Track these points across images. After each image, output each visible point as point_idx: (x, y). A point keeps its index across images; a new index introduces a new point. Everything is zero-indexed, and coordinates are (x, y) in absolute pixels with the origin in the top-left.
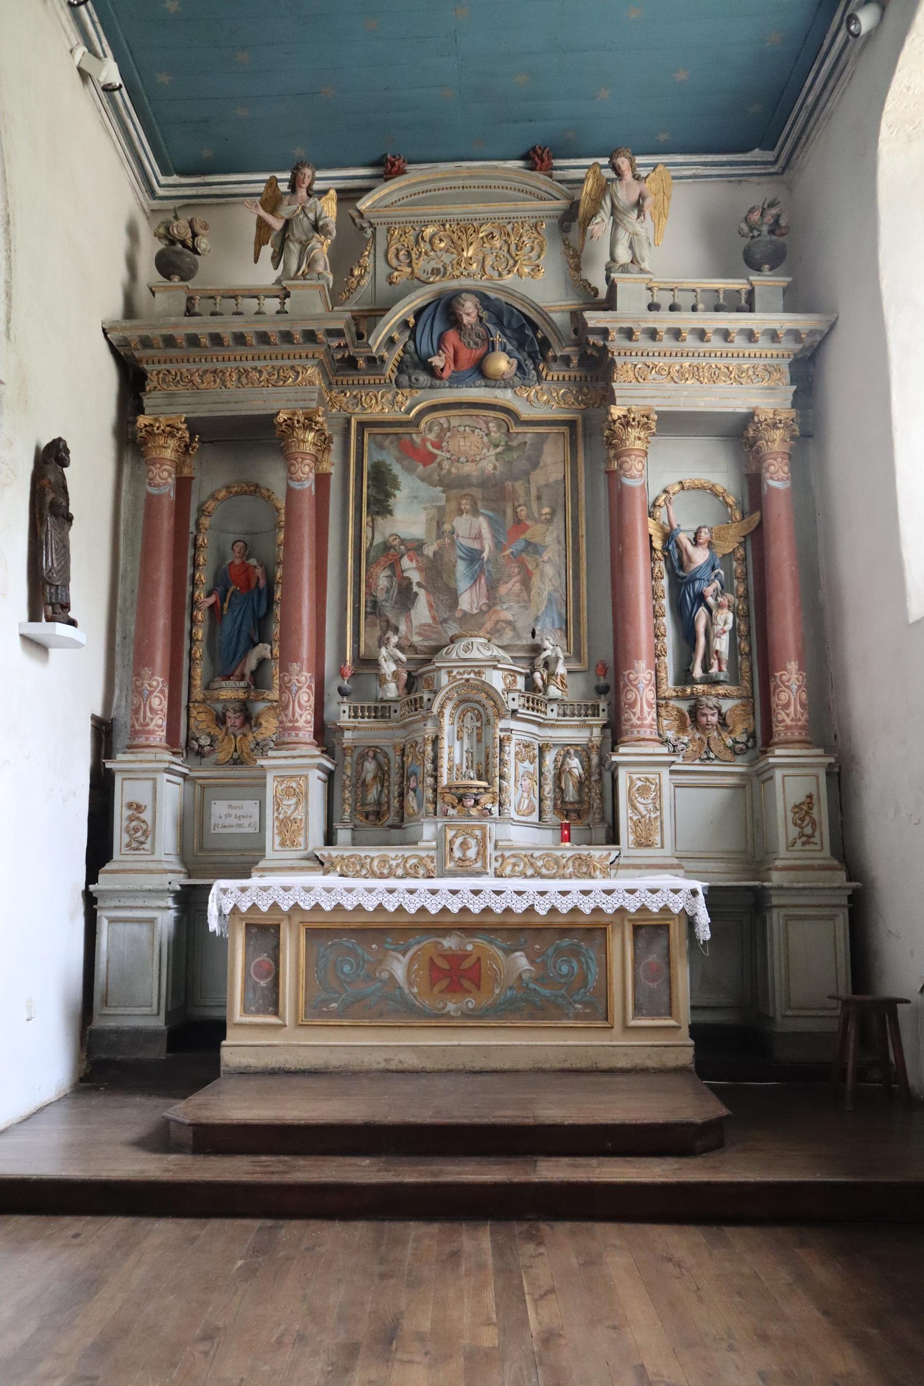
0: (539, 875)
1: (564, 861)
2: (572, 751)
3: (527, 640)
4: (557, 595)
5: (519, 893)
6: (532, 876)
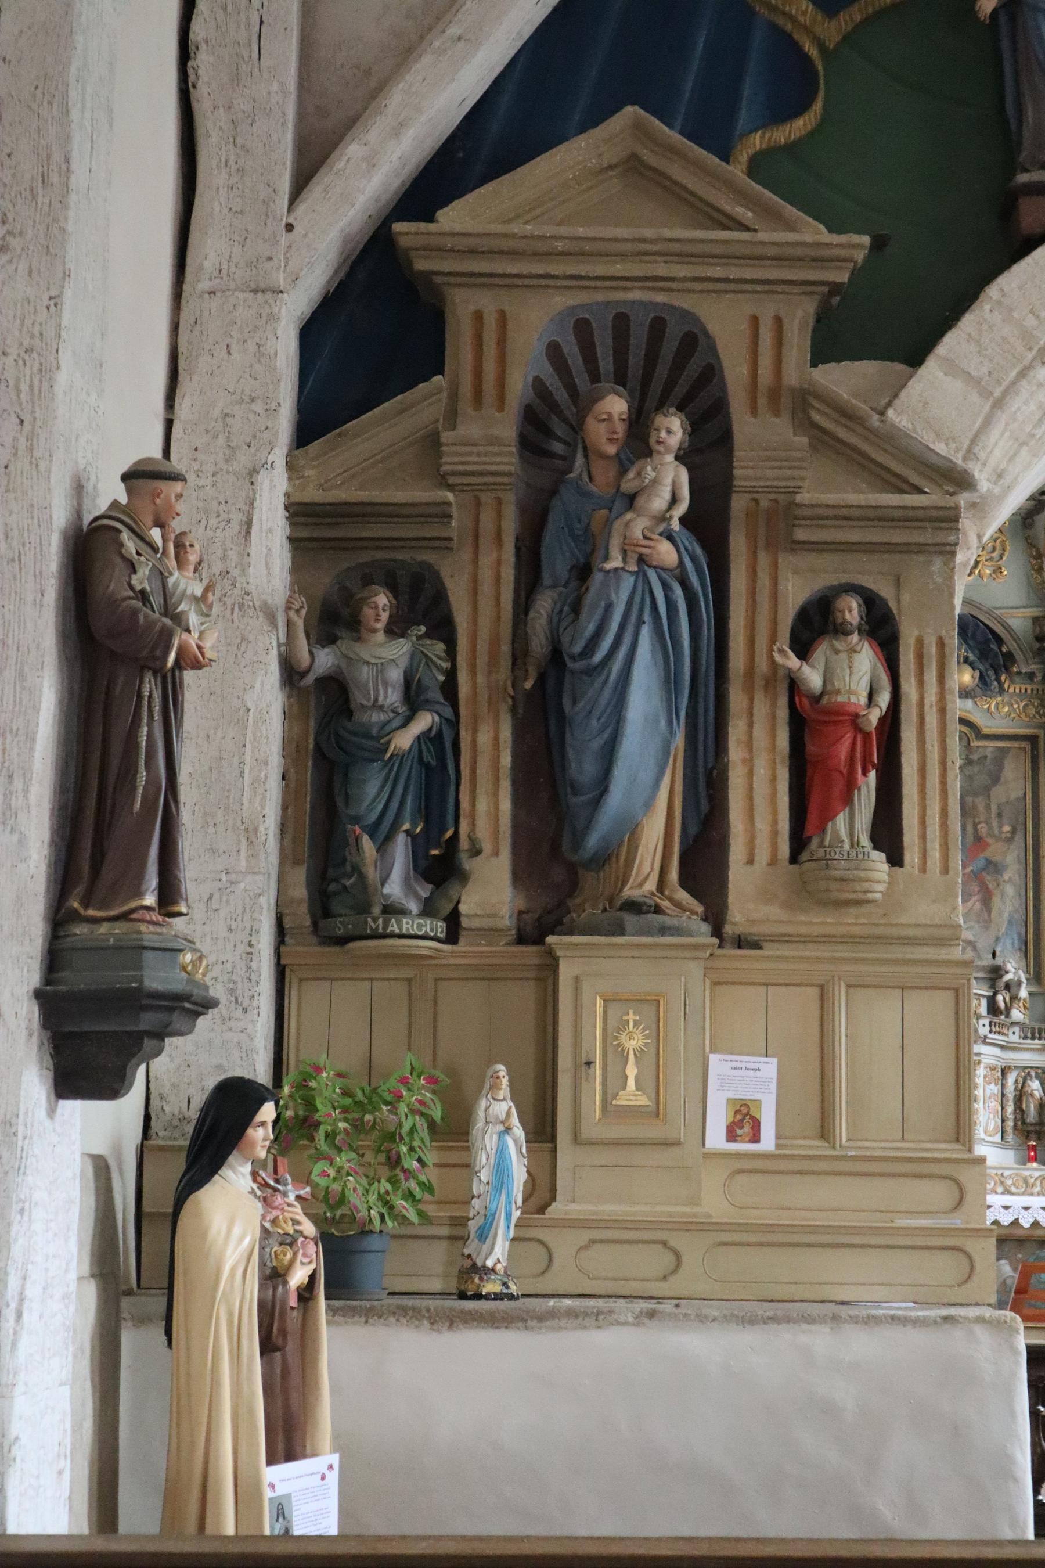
0: (1007, 1192)
1: (1032, 1180)
2: (1033, 1074)
3: (987, 961)
4: (1016, 916)
5: (1006, 1208)
6: (1003, 1193)
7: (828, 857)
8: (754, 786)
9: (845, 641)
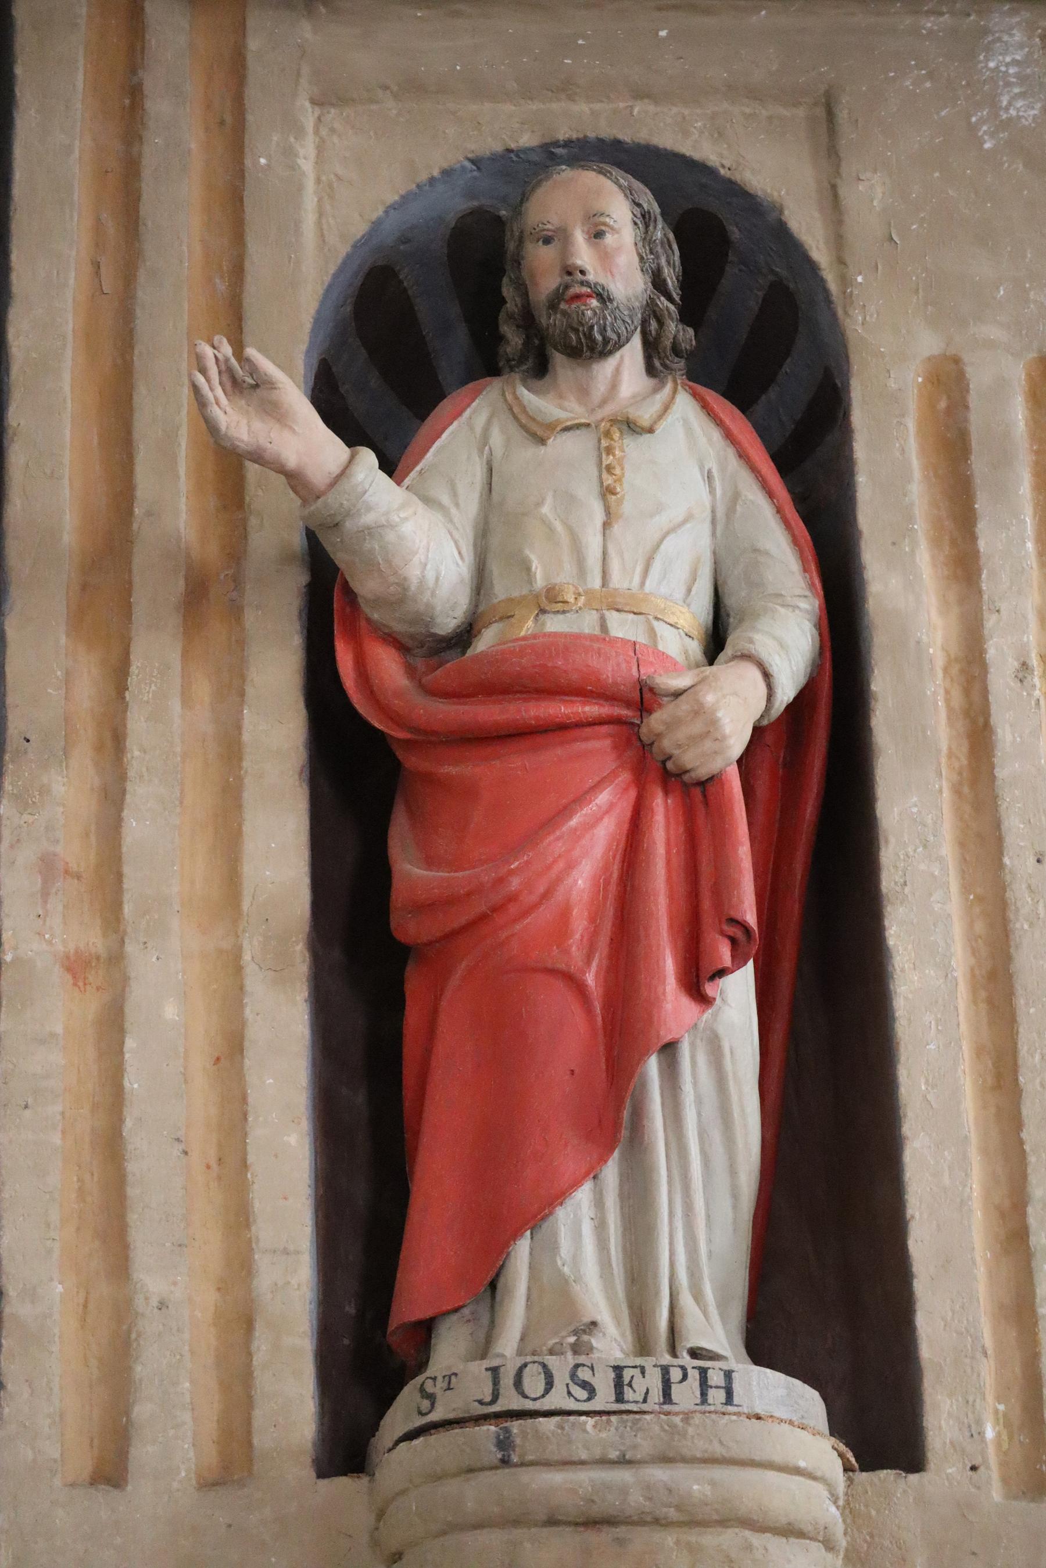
7: (511, 1401)
8: (132, 1083)
9: (583, 392)
